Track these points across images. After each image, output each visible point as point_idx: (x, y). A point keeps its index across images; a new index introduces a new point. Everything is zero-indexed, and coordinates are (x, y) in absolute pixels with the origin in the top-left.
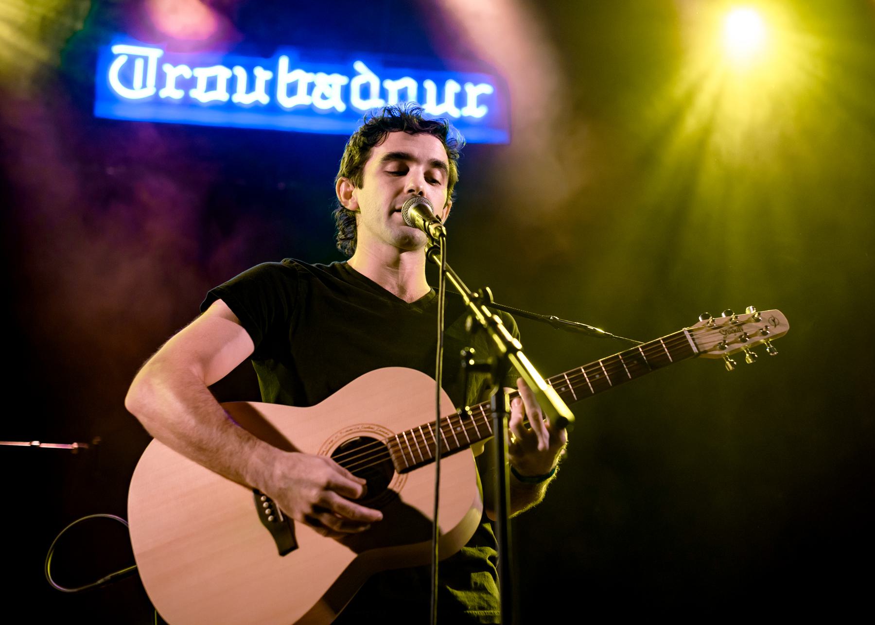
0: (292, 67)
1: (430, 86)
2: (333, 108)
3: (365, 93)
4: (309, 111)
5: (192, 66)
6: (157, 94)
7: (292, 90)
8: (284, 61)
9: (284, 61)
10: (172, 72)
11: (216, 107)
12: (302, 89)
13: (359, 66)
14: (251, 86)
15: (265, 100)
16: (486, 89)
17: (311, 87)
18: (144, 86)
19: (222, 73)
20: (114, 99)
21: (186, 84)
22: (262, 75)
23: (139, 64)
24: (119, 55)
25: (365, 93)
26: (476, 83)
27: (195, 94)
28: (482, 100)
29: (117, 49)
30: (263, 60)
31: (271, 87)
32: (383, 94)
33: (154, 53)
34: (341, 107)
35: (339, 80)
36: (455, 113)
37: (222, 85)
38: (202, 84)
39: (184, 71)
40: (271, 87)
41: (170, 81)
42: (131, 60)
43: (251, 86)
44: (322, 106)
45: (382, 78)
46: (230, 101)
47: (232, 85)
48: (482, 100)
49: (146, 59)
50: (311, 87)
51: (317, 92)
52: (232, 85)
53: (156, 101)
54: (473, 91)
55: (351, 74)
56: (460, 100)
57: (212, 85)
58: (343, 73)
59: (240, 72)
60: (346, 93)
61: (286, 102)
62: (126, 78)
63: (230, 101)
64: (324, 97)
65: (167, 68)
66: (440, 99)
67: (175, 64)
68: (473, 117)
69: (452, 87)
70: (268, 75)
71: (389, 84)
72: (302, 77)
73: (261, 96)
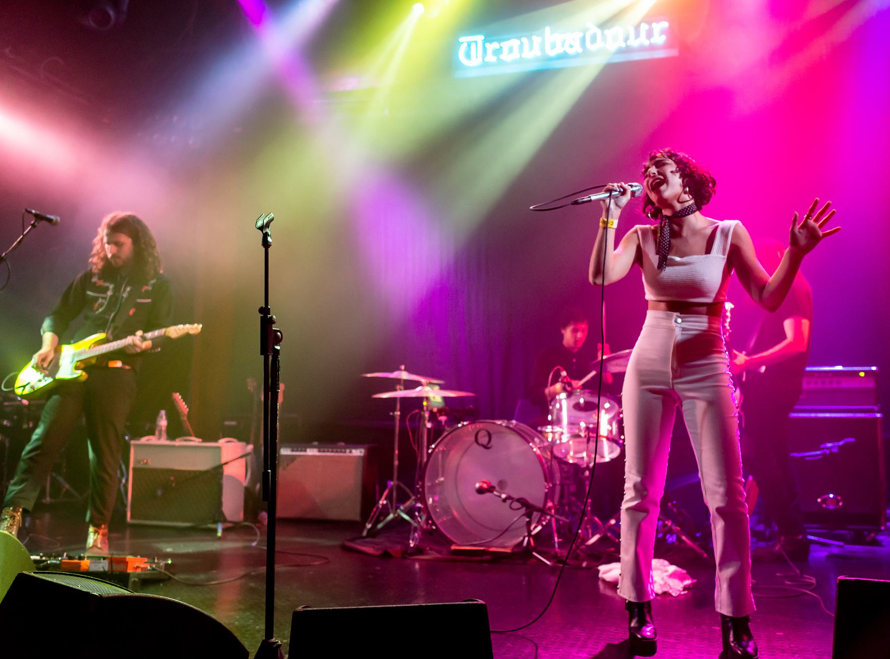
5: (499, 41)
6: (483, 60)
7: (553, 46)
14: (531, 48)
19: (514, 43)
21: (498, 52)
22: (536, 39)
23: (473, 45)
28: (663, 32)
36: (647, 43)
37: (516, 50)
39: (495, 45)
42: (469, 45)
43: (531, 48)
49: (476, 42)
53: (485, 65)
56: (650, 34)
57: (511, 50)
64: (571, 46)
65: (487, 45)
67: (491, 42)
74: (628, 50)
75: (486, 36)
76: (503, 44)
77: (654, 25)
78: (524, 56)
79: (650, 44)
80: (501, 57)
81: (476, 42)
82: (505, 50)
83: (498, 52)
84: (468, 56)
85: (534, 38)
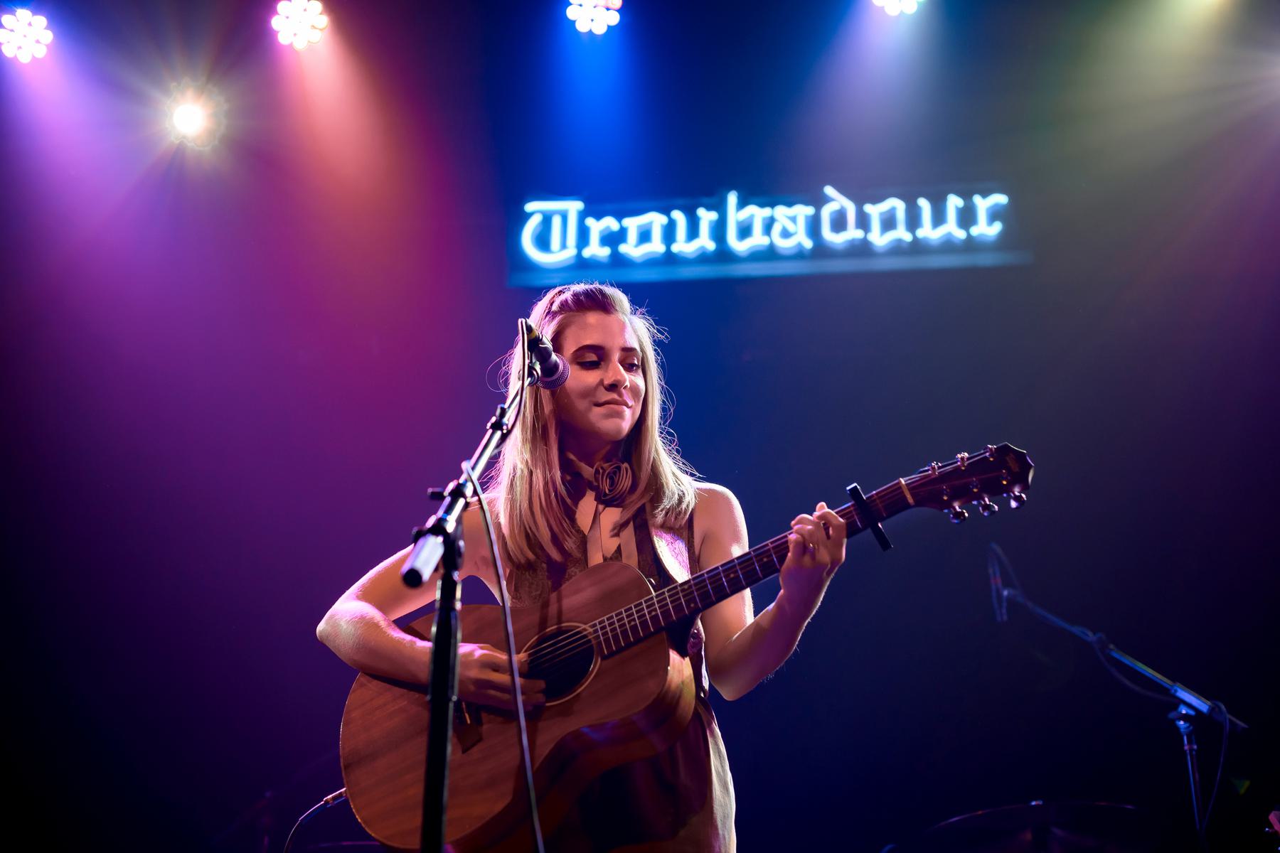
0: (742, 204)
1: (924, 204)
2: (800, 245)
3: (839, 223)
4: (770, 253)
5: (619, 216)
6: (579, 255)
7: (745, 231)
8: (732, 198)
9: (732, 198)
10: (597, 227)
11: (652, 262)
12: (758, 227)
13: (829, 190)
14: (693, 233)
15: (711, 246)
16: (1001, 199)
17: (769, 225)
18: (564, 246)
19: (656, 220)
20: (529, 266)
21: (614, 239)
22: (706, 217)
23: (556, 222)
24: (531, 215)
25: (839, 223)
26: (985, 194)
27: (623, 248)
28: (994, 215)
29: (530, 207)
30: (705, 200)
31: (719, 231)
32: (863, 222)
33: (574, 207)
34: (808, 244)
35: (803, 211)
36: (961, 234)
37: (657, 234)
38: (632, 236)
39: (610, 223)
40: (719, 231)
41: (594, 237)
42: (547, 219)
43: (693, 233)
44: (784, 245)
45: (859, 202)
46: (668, 251)
47: (669, 233)
48: (994, 215)
50: (769, 225)
51: (776, 229)
52: (669, 233)
54: (983, 204)
55: (819, 201)
56: (967, 218)
57: (645, 236)
58: (806, 203)
59: (678, 216)
60: (814, 227)
61: (739, 246)
62: (543, 241)
63: (668, 251)
64: (786, 234)
65: (590, 221)
66: (939, 219)
68: (986, 236)
69: (954, 202)
70: (714, 216)
71: (868, 208)
72: (756, 213)
73: (705, 242)
74: (918, 247)
75: (587, 201)
77: (977, 199)
78: (675, 248)
79: (969, 235)
80: (623, 248)
82: (632, 236)
83: (614, 239)
85: (701, 212)
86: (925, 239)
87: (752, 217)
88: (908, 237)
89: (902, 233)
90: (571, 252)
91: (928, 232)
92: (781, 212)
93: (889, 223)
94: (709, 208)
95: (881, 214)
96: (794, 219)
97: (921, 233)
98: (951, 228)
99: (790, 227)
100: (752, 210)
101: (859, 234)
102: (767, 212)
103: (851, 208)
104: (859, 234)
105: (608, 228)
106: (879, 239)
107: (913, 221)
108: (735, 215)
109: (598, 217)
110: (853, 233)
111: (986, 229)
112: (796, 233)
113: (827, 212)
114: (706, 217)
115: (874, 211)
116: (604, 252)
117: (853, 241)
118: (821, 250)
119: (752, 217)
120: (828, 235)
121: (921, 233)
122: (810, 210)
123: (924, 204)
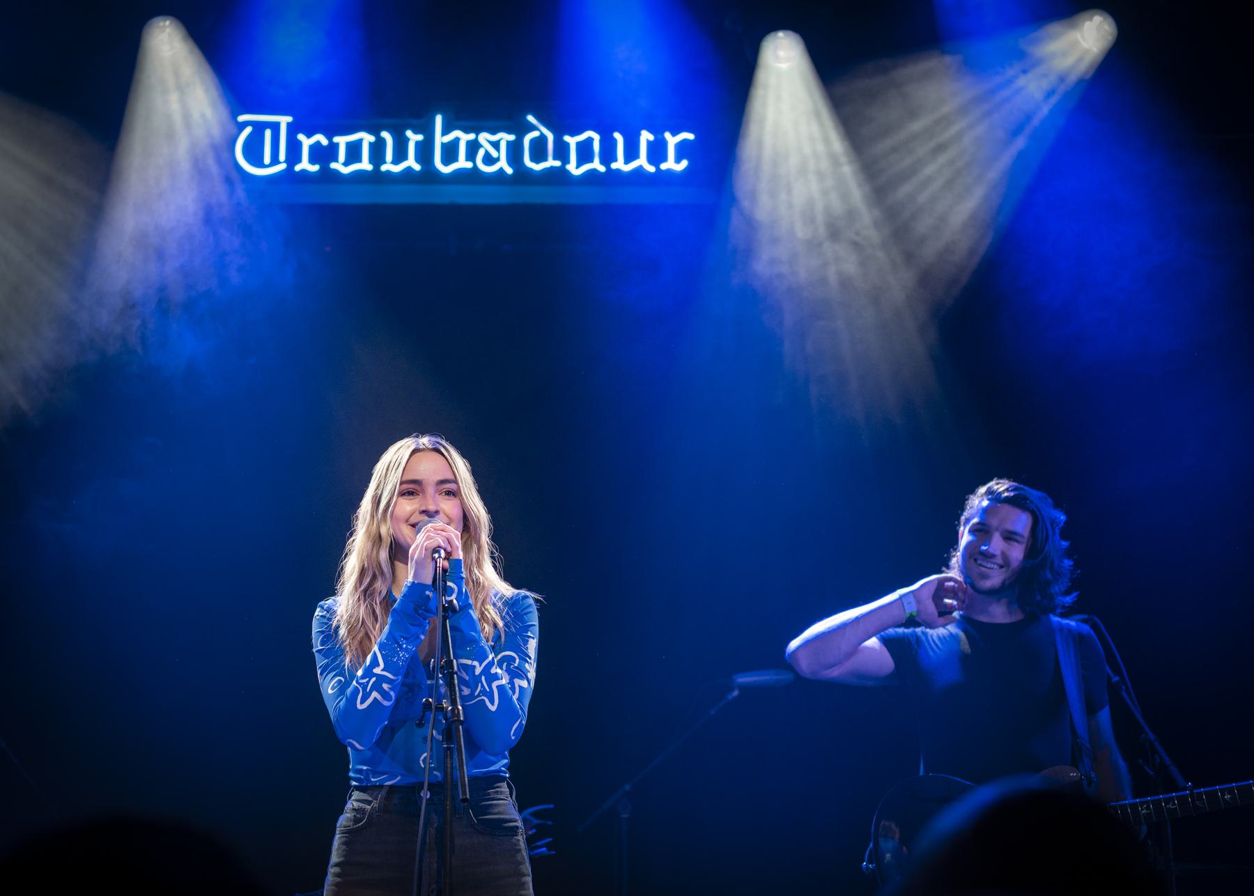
1: (618, 136)
2: (501, 170)
3: (539, 151)
4: (473, 176)
7: (450, 153)
8: (439, 119)
9: (439, 119)
10: (306, 142)
11: (359, 176)
13: (531, 118)
14: (400, 156)
15: (417, 167)
17: (473, 147)
19: (367, 138)
22: (414, 138)
25: (539, 151)
26: (675, 133)
27: (333, 165)
28: (683, 150)
30: (414, 122)
31: (425, 152)
32: (562, 152)
33: (284, 120)
34: (509, 171)
35: (505, 138)
36: (651, 169)
39: (321, 139)
40: (425, 152)
43: (400, 156)
47: (377, 152)
48: (683, 150)
49: (275, 127)
50: (473, 147)
51: (481, 153)
52: (377, 152)
53: (289, 176)
54: (672, 140)
56: (657, 152)
57: (354, 153)
59: (386, 135)
60: (515, 152)
61: (446, 170)
64: (489, 160)
65: (301, 137)
66: (631, 154)
69: (646, 136)
70: (420, 137)
71: (567, 138)
73: (412, 163)
76: (336, 139)
77: (667, 135)
78: (384, 168)
80: (333, 165)
81: (275, 127)
83: (323, 155)
84: (256, 160)
85: (409, 133)
86: (618, 171)
87: (457, 140)
88: (602, 169)
89: (597, 165)
90: (282, 166)
91: (619, 164)
92: (484, 137)
93: (585, 153)
94: (416, 132)
95: (578, 144)
96: (496, 145)
97: (614, 166)
98: (642, 161)
99: (494, 154)
100: (456, 133)
101: (558, 163)
102: (472, 136)
103: (550, 137)
104: (558, 163)
105: (318, 143)
106: (573, 169)
107: (608, 155)
108: (440, 139)
109: (309, 136)
110: (552, 163)
111: (673, 164)
112: (498, 159)
113: (527, 139)
114: (414, 138)
115: (572, 141)
116: (315, 168)
117: (552, 168)
118: (523, 175)
119: (457, 140)
120: (527, 162)
121: (614, 166)
122: (512, 137)
123: (618, 136)
